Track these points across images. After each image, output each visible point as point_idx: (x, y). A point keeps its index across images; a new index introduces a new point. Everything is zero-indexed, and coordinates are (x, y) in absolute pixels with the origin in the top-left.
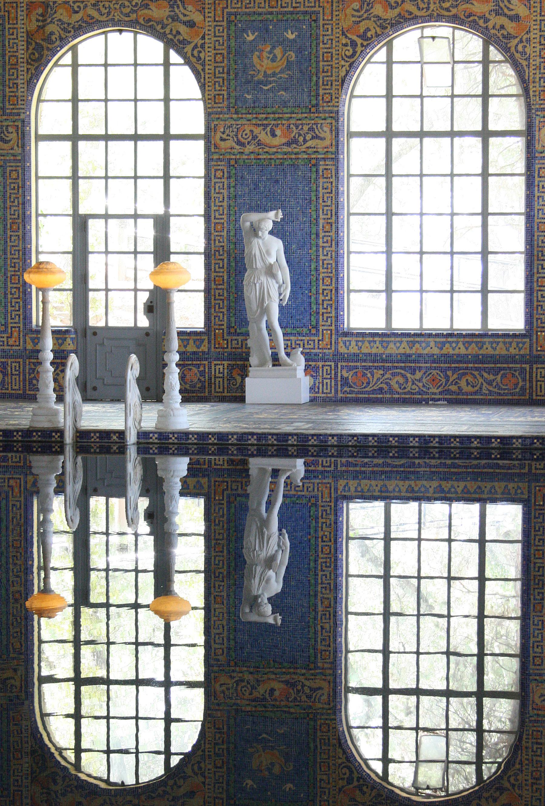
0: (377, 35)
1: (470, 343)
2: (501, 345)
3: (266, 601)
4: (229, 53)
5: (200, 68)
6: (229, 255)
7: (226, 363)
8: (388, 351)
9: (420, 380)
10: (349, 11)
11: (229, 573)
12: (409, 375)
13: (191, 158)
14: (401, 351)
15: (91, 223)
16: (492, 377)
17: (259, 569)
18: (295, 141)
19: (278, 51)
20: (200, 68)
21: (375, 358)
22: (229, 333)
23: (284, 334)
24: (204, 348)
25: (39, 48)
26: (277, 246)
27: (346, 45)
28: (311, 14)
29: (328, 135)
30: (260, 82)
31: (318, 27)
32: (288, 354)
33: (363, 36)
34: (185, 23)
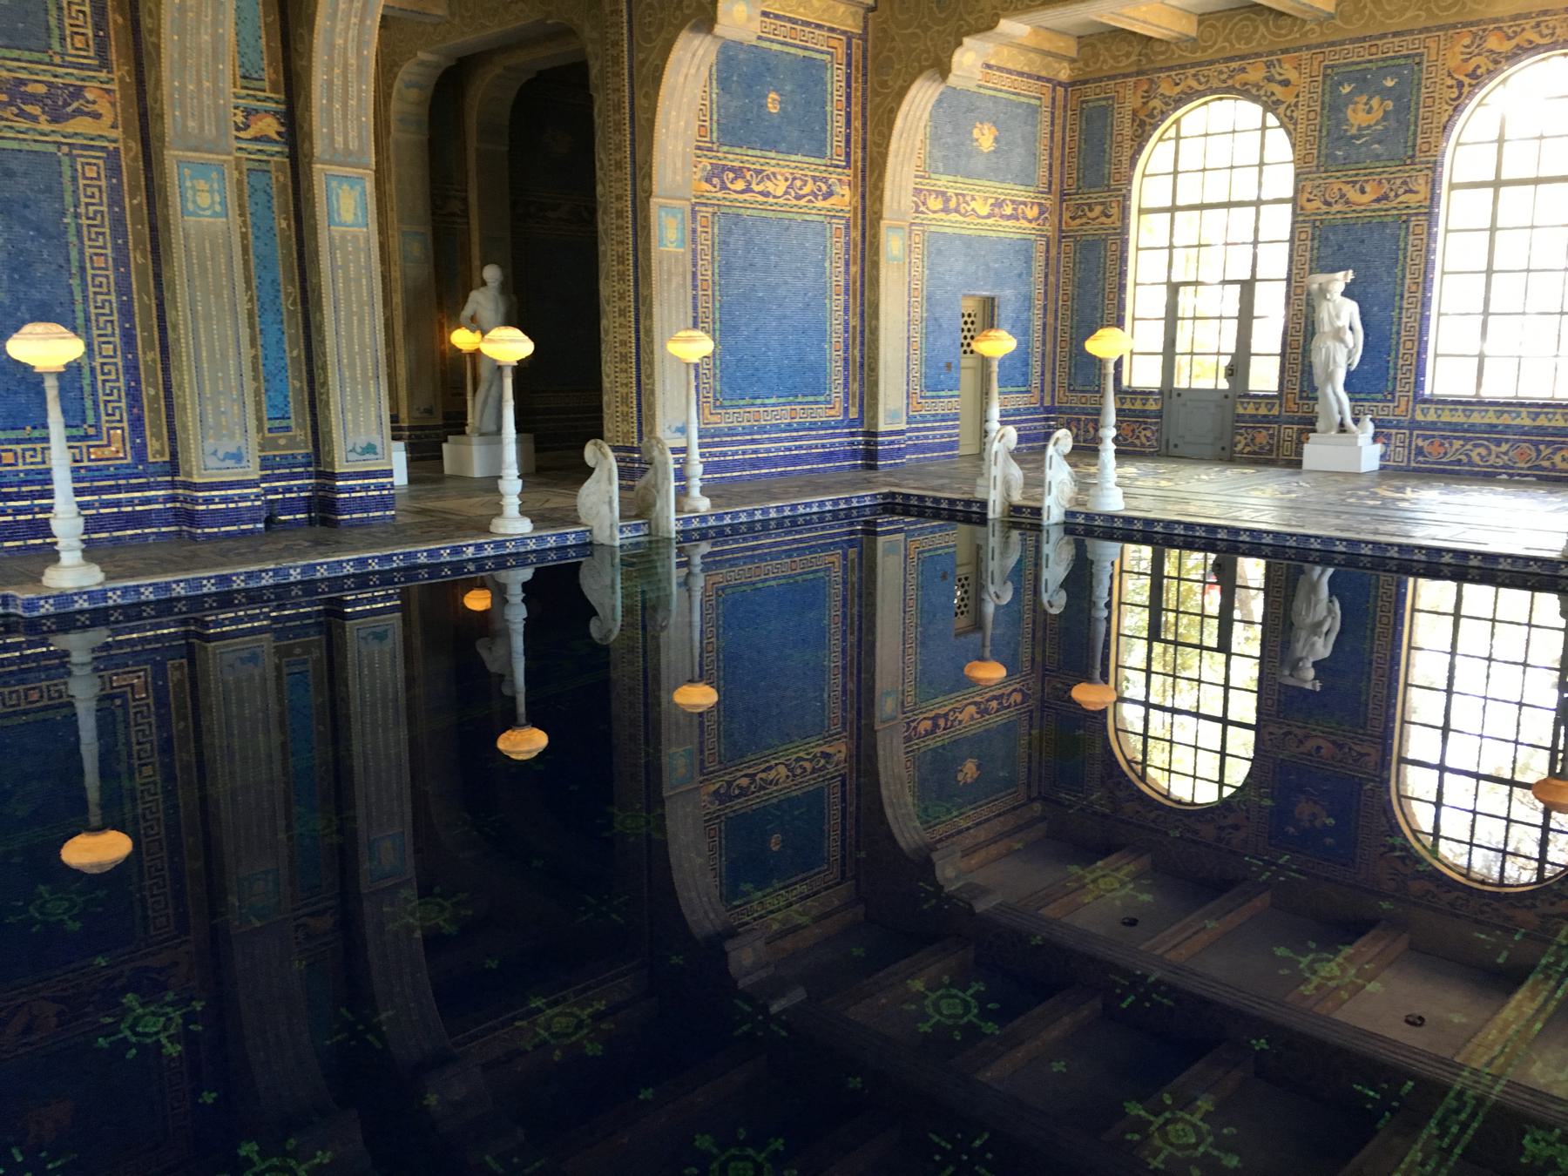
0: (1489, 72)
8: (1471, 421)
9: (1505, 453)
10: (1458, 49)
12: (1493, 447)
13: (1279, 222)
17: (1303, 634)
18: (1385, 197)
19: (1375, 102)
20: (1291, 127)
21: (1455, 427)
22: (1301, 398)
24: (1275, 411)
25: (1142, 124)
26: (1349, 311)
32: (1356, 421)
33: (1473, 75)
34: (1280, 83)
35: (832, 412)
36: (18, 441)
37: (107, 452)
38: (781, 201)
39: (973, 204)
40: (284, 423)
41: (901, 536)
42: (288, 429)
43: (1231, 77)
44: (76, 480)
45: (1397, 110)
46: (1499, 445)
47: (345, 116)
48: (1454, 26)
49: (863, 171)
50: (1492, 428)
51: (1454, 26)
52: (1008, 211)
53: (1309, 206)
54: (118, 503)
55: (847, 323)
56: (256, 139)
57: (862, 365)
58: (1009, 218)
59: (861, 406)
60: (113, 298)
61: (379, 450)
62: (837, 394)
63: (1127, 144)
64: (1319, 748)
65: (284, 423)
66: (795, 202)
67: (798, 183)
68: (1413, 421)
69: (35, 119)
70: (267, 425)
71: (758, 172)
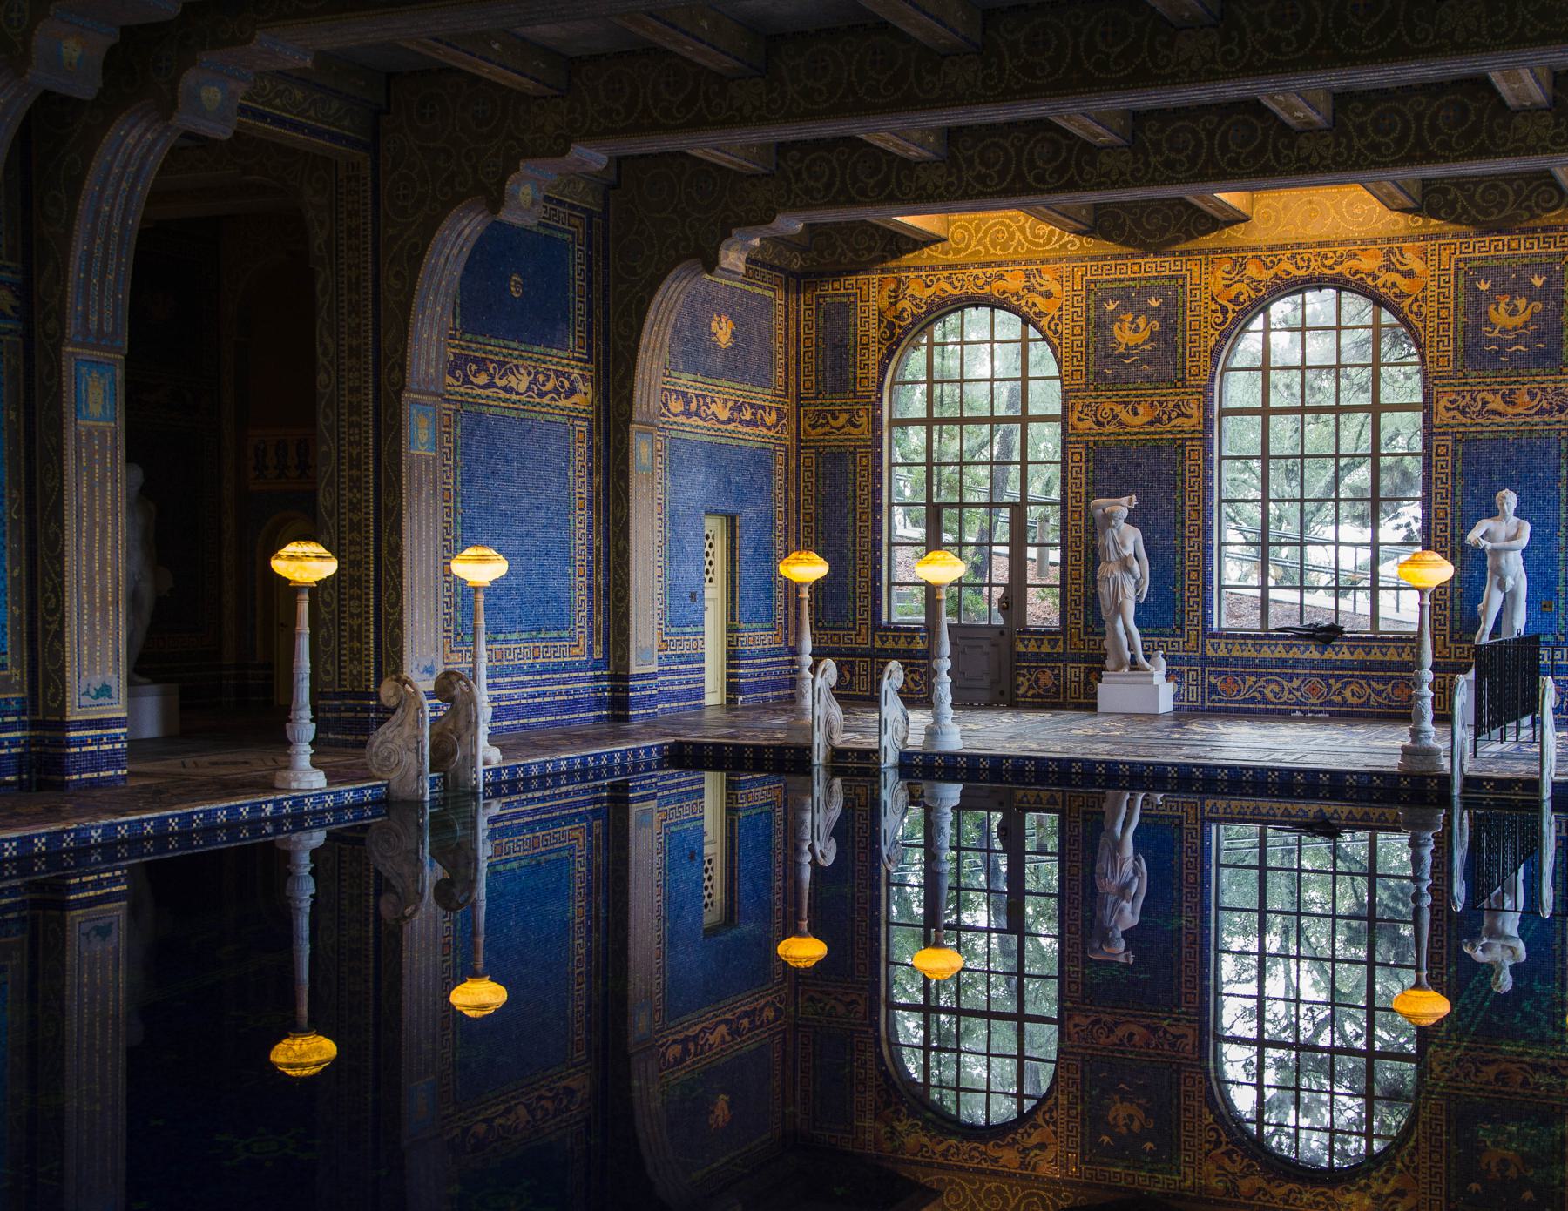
1: (1356, 647)
2: (1392, 650)
3: (1119, 935)
4: (1088, 325)
5: (1056, 341)
6: (1086, 546)
7: (1082, 666)
8: (1261, 655)
9: (1298, 689)
10: (1219, 274)
11: (1084, 899)
13: (1046, 441)
14: (1277, 655)
15: (945, 512)
16: (1381, 687)
17: (1111, 898)
18: (1159, 420)
21: (1246, 663)
22: (1086, 633)
23: (1142, 635)
27: (1215, 311)
28: (1177, 277)
29: (1195, 413)
30: (1122, 356)
31: (1184, 293)
32: (1148, 658)
34: (1041, 294)
35: (577, 651)
38: (523, 398)
39: (713, 407)
41: (653, 804)
43: (987, 283)
45: (1163, 332)
46: (1290, 681)
48: (1214, 251)
49: (606, 365)
50: (1283, 663)
51: (1214, 251)
52: (748, 416)
53: (1081, 425)
55: (590, 542)
57: (607, 594)
58: (748, 423)
59: (606, 643)
61: (114, 693)
62: (582, 628)
63: (874, 347)
64: (1132, 1035)
66: (537, 400)
67: (541, 378)
68: (1204, 657)
71: (501, 364)
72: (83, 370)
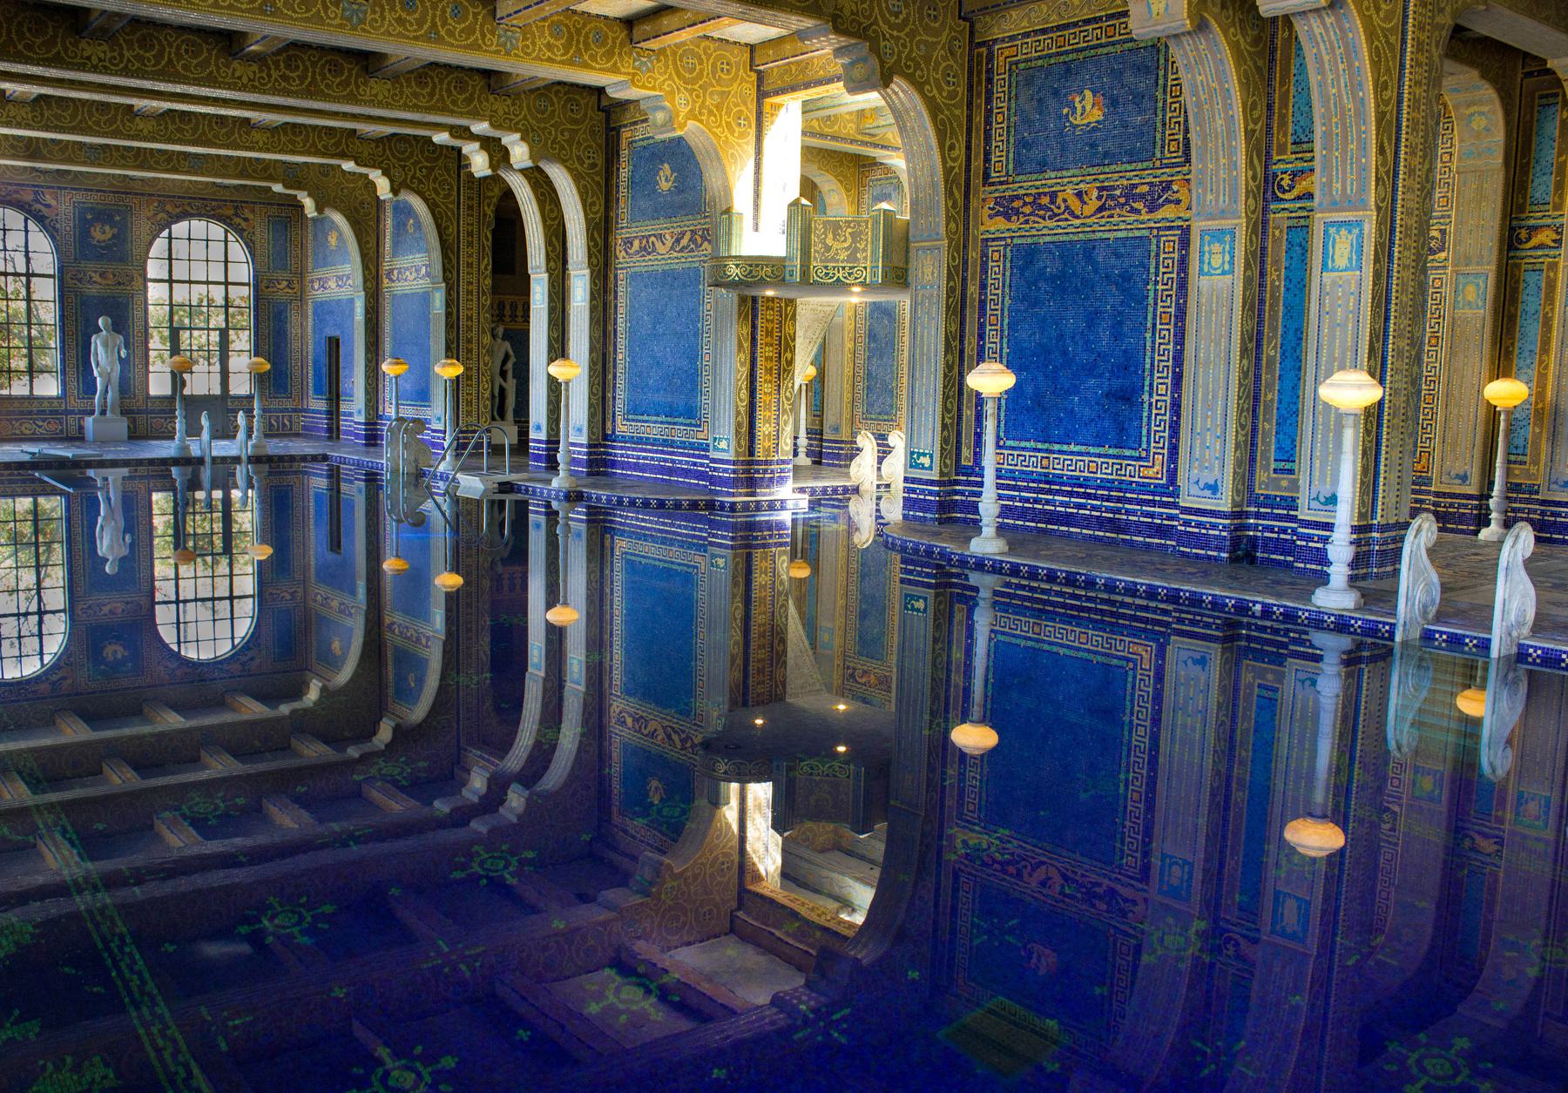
36: (1100, 456)
37: (1151, 472)
40: (1288, 466)
42: (1291, 471)
44: (998, 477)
47: (1344, 161)
54: (1152, 515)
56: (1299, 198)
60: (1171, 347)
65: (1288, 466)
69: (1138, 212)
70: (1273, 466)
72: (1332, 230)
